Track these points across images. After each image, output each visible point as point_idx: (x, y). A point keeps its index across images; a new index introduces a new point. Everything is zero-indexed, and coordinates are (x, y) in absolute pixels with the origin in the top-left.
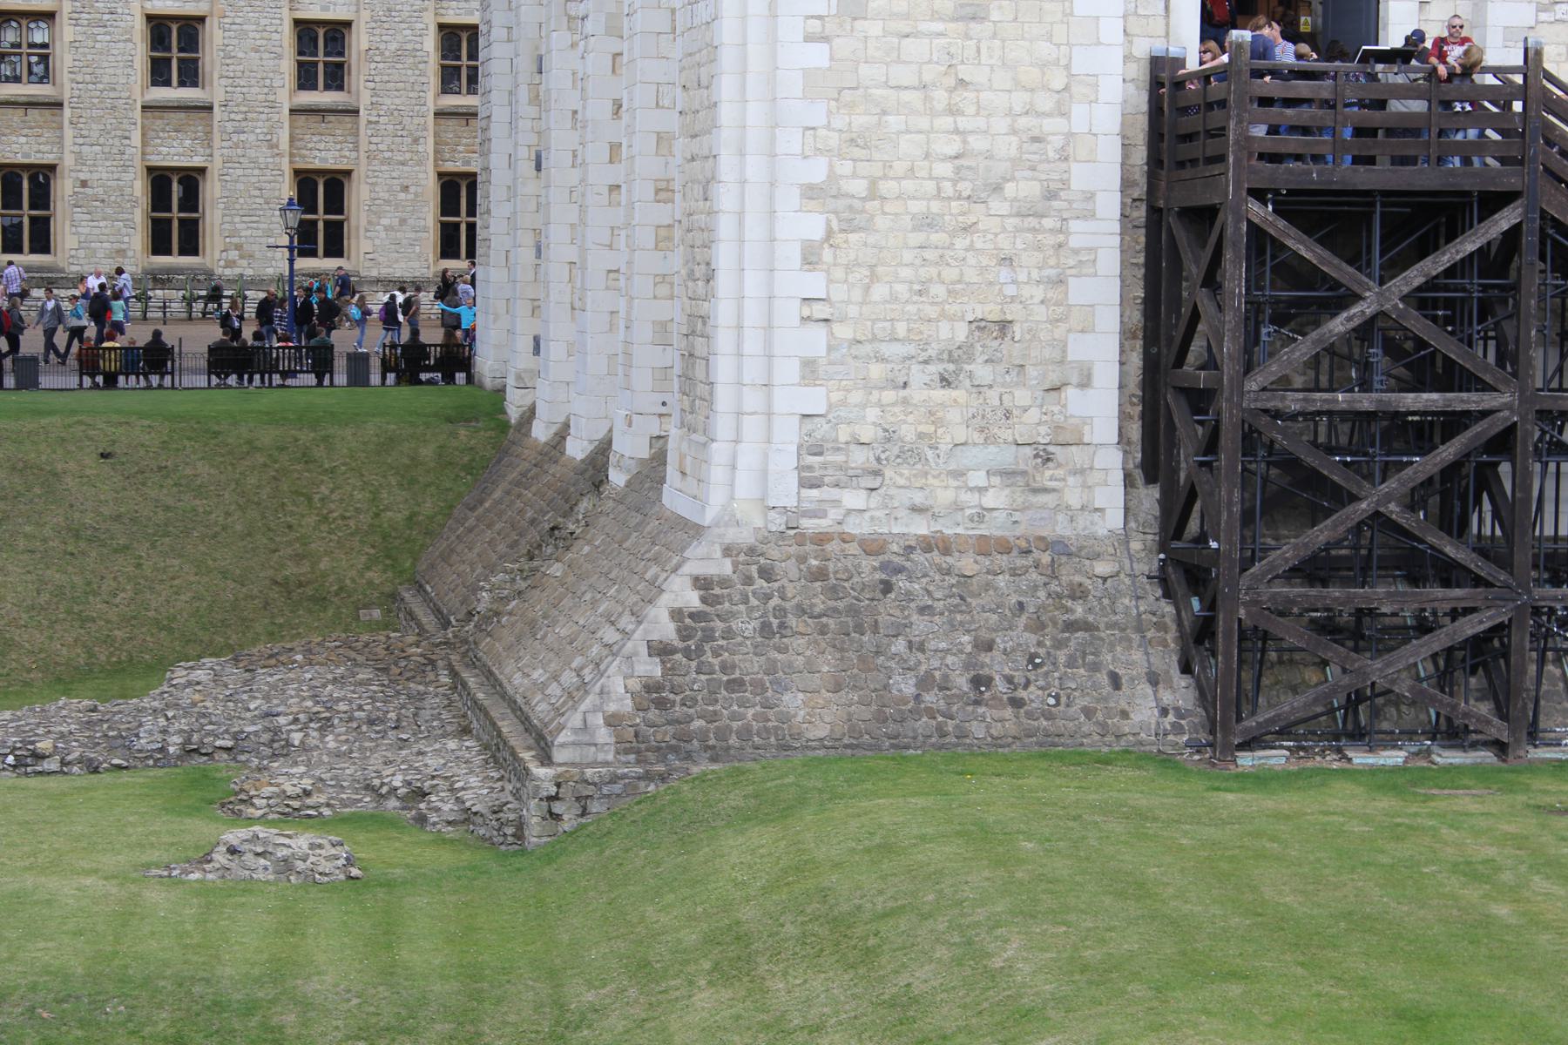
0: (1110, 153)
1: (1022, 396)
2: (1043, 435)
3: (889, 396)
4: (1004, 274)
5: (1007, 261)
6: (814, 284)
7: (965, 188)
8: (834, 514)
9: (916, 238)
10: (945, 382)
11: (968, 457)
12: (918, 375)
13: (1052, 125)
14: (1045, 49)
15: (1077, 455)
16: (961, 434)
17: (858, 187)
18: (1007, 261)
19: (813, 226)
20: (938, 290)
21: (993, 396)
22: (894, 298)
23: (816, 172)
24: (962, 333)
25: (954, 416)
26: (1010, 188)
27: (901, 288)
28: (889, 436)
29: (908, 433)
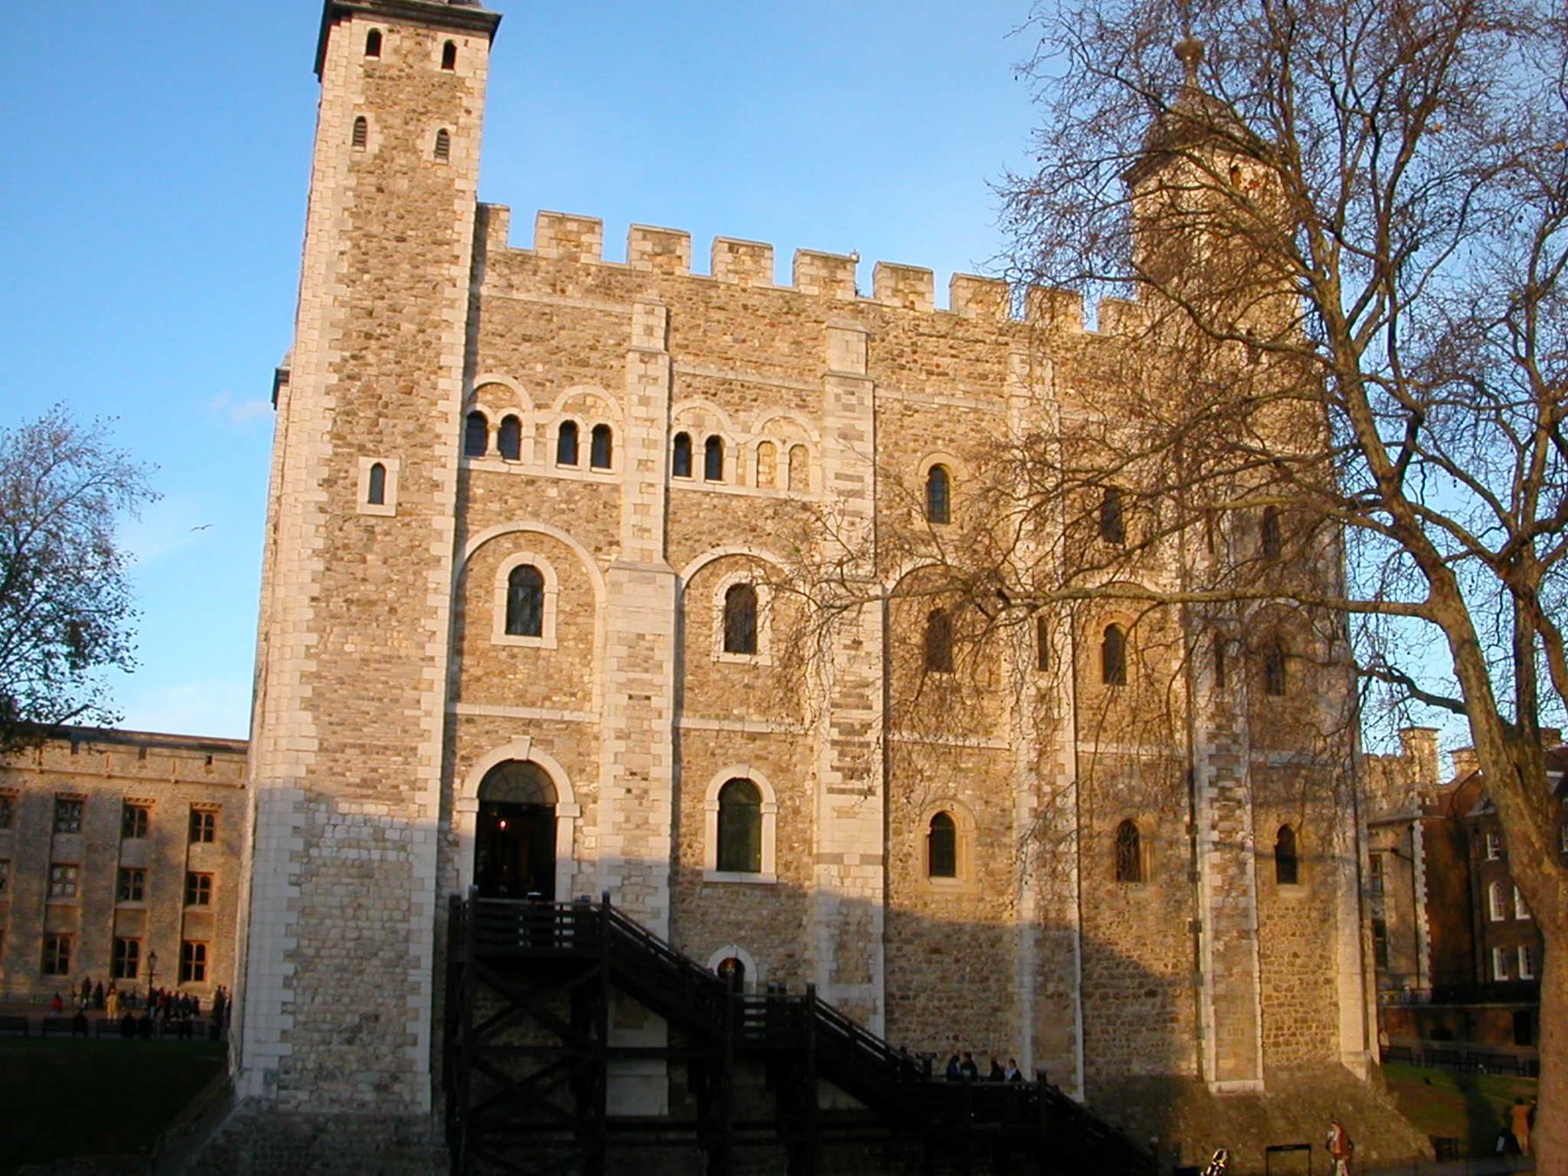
0: (428, 938)
1: (384, 1049)
2: (393, 1068)
3: (322, 1048)
4: (377, 993)
5: (378, 987)
6: (288, 996)
7: (360, 952)
8: (294, 1103)
9: (337, 975)
10: (350, 1042)
11: (358, 1077)
12: (336, 1039)
13: (400, 926)
14: (398, 892)
15: (408, 1076)
16: (355, 1066)
17: (311, 952)
18: (378, 987)
19: (289, 968)
20: (346, 1000)
21: (371, 1049)
22: (325, 1003)
23: (291, 944)
24: (357, 1020)
25: (352, 1057)
26: (381, 954)
27: (329, 999)
28: (321, 1067)
29: (330, 1064)
